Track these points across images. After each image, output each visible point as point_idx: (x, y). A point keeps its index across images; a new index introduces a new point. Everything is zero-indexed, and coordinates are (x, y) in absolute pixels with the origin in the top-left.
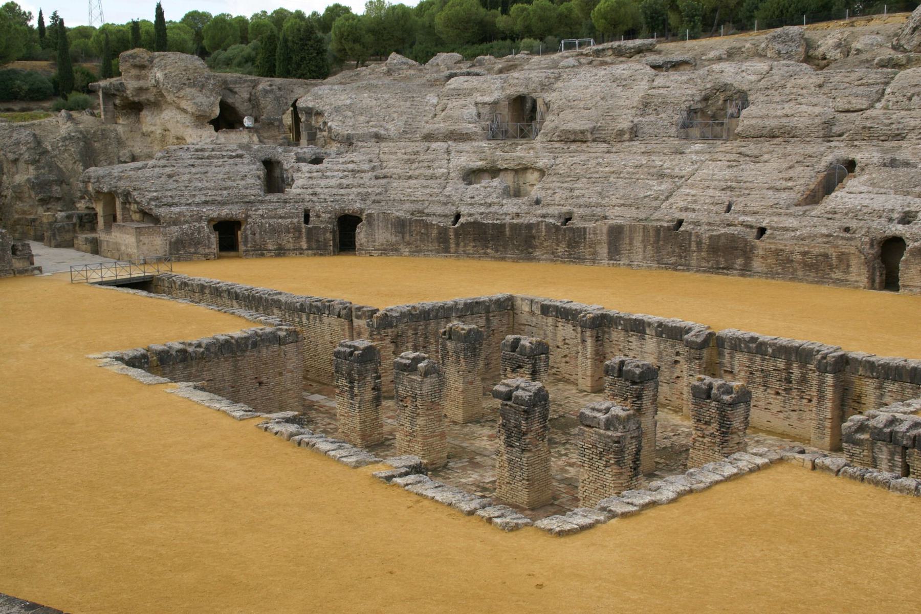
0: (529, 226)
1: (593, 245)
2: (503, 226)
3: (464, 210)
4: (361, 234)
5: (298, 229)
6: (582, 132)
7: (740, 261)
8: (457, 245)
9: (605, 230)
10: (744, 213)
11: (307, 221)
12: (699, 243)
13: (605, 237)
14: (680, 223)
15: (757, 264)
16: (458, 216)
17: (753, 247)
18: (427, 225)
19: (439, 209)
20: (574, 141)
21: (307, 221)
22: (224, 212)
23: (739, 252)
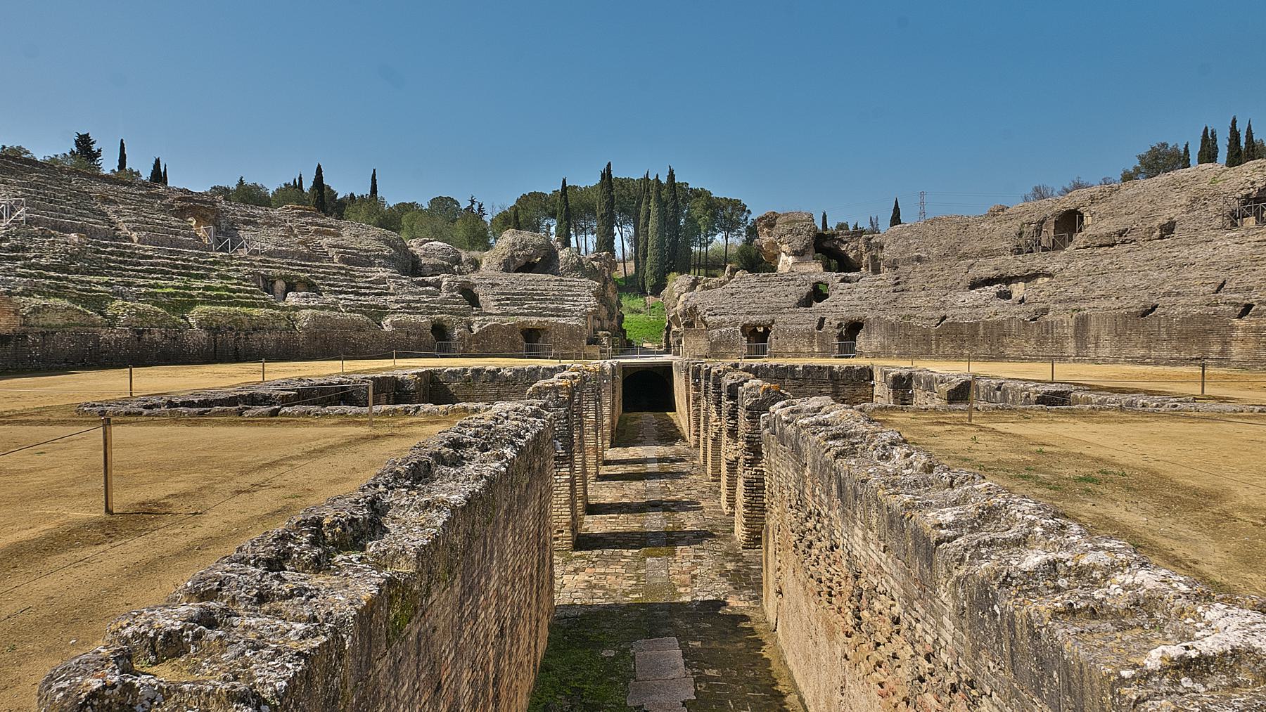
0: (1000, 324)
1: (1060, 341)
2: (977, 324)
3: (949, 313)
4: (861, 340)
5: (812, 335)
6: (1109, 235)
7: (1216, 348)
8: (938, 346)
9: (1072, 323)
10: (1237, 291)
11: (820, 326)
12: (1169, 328)
13: (1071, 331)
14: (1153, 308)
15: (1236, 351)
16: (945, 318)
17: (1233, 328)
18: (911, 326)
19: (929, 313)
20: (1101, 246)
21: (820, 326)
22: (754, 319)
23: (1213, 338)
